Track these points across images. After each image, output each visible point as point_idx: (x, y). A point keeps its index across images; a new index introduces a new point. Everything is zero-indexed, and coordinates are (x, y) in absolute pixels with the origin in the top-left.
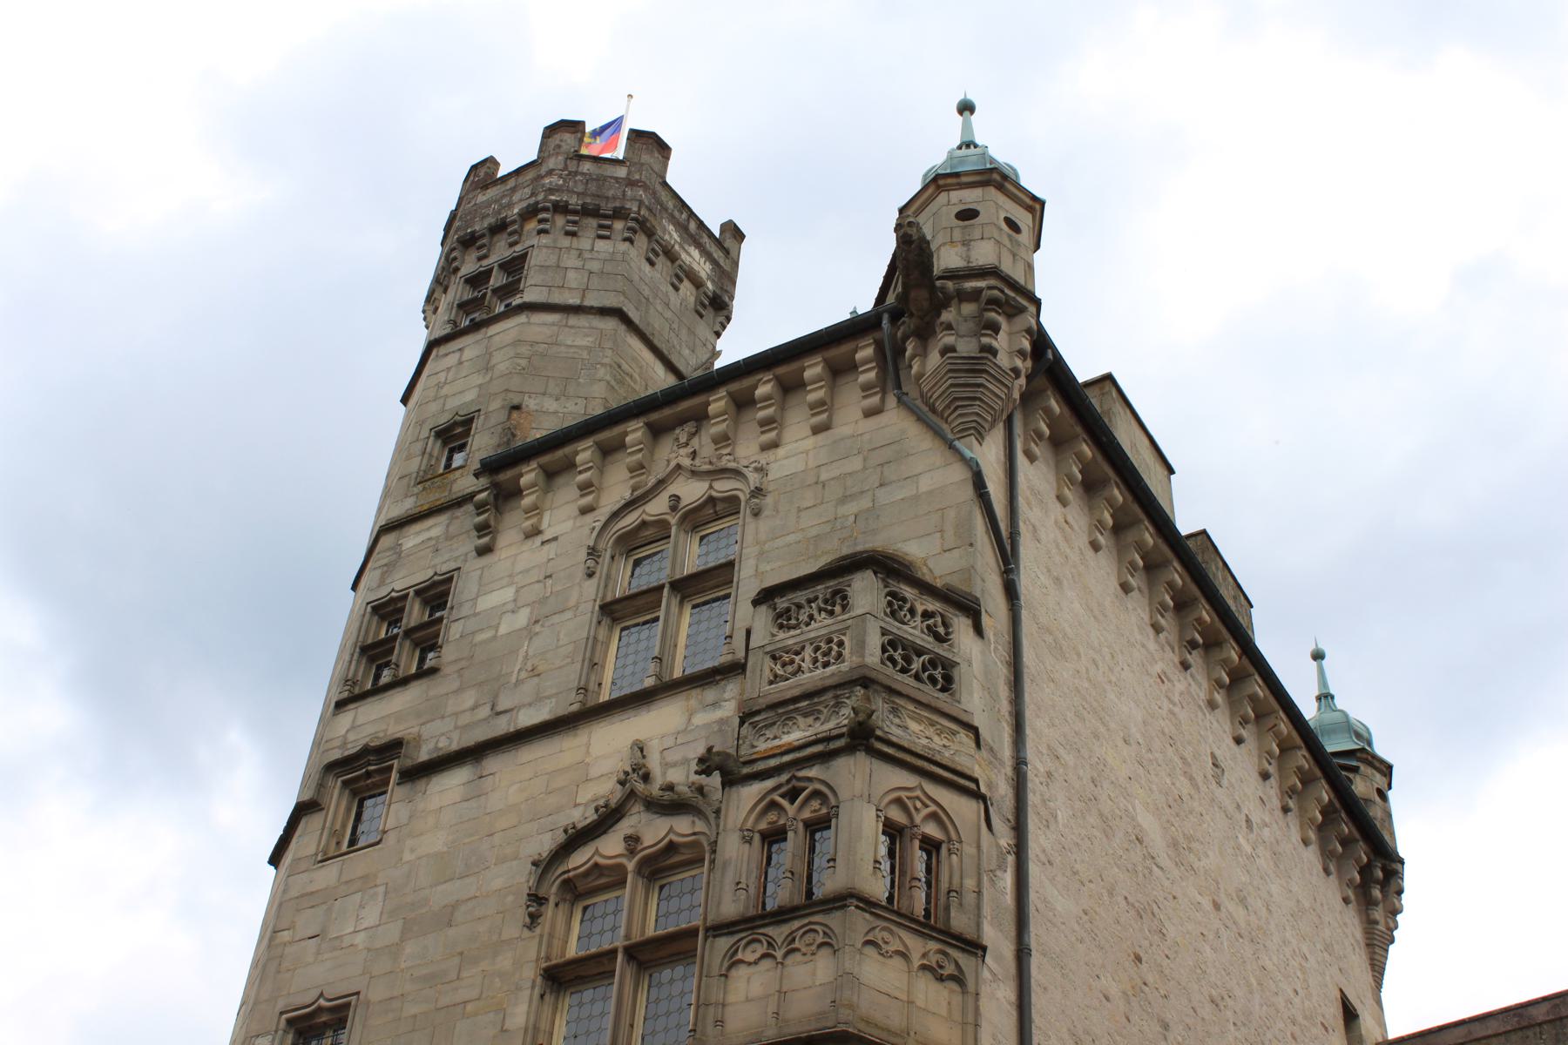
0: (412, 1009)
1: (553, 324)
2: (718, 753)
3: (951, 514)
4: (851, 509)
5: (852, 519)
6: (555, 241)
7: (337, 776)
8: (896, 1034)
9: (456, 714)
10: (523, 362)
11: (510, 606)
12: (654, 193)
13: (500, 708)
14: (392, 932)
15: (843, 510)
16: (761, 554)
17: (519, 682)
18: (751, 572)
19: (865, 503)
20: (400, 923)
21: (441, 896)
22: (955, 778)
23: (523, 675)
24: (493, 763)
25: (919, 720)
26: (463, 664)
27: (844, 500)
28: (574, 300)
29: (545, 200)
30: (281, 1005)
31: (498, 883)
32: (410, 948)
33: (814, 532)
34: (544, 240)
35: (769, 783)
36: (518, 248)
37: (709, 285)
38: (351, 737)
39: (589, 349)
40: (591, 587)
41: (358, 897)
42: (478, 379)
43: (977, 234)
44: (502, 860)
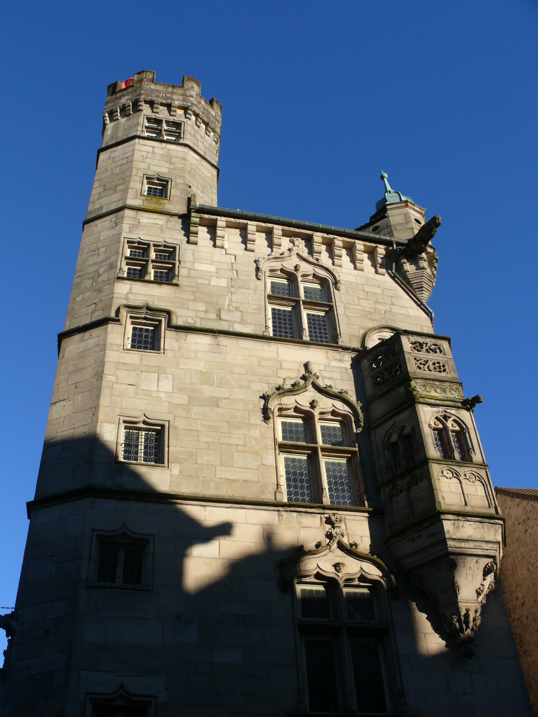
4: (383, 308)
5: (383, 312)
14: (183, 399)
15: (378, 306)
16: (345, 308)
18: (343, 313)
19: (387, 308)
21: (208, 391)
24: (224, 340)
26: (196, 290)
27: (377, 302)
30: (118, 411)
31: (241, 397)
33: (368, 310)
44: (242, 387)
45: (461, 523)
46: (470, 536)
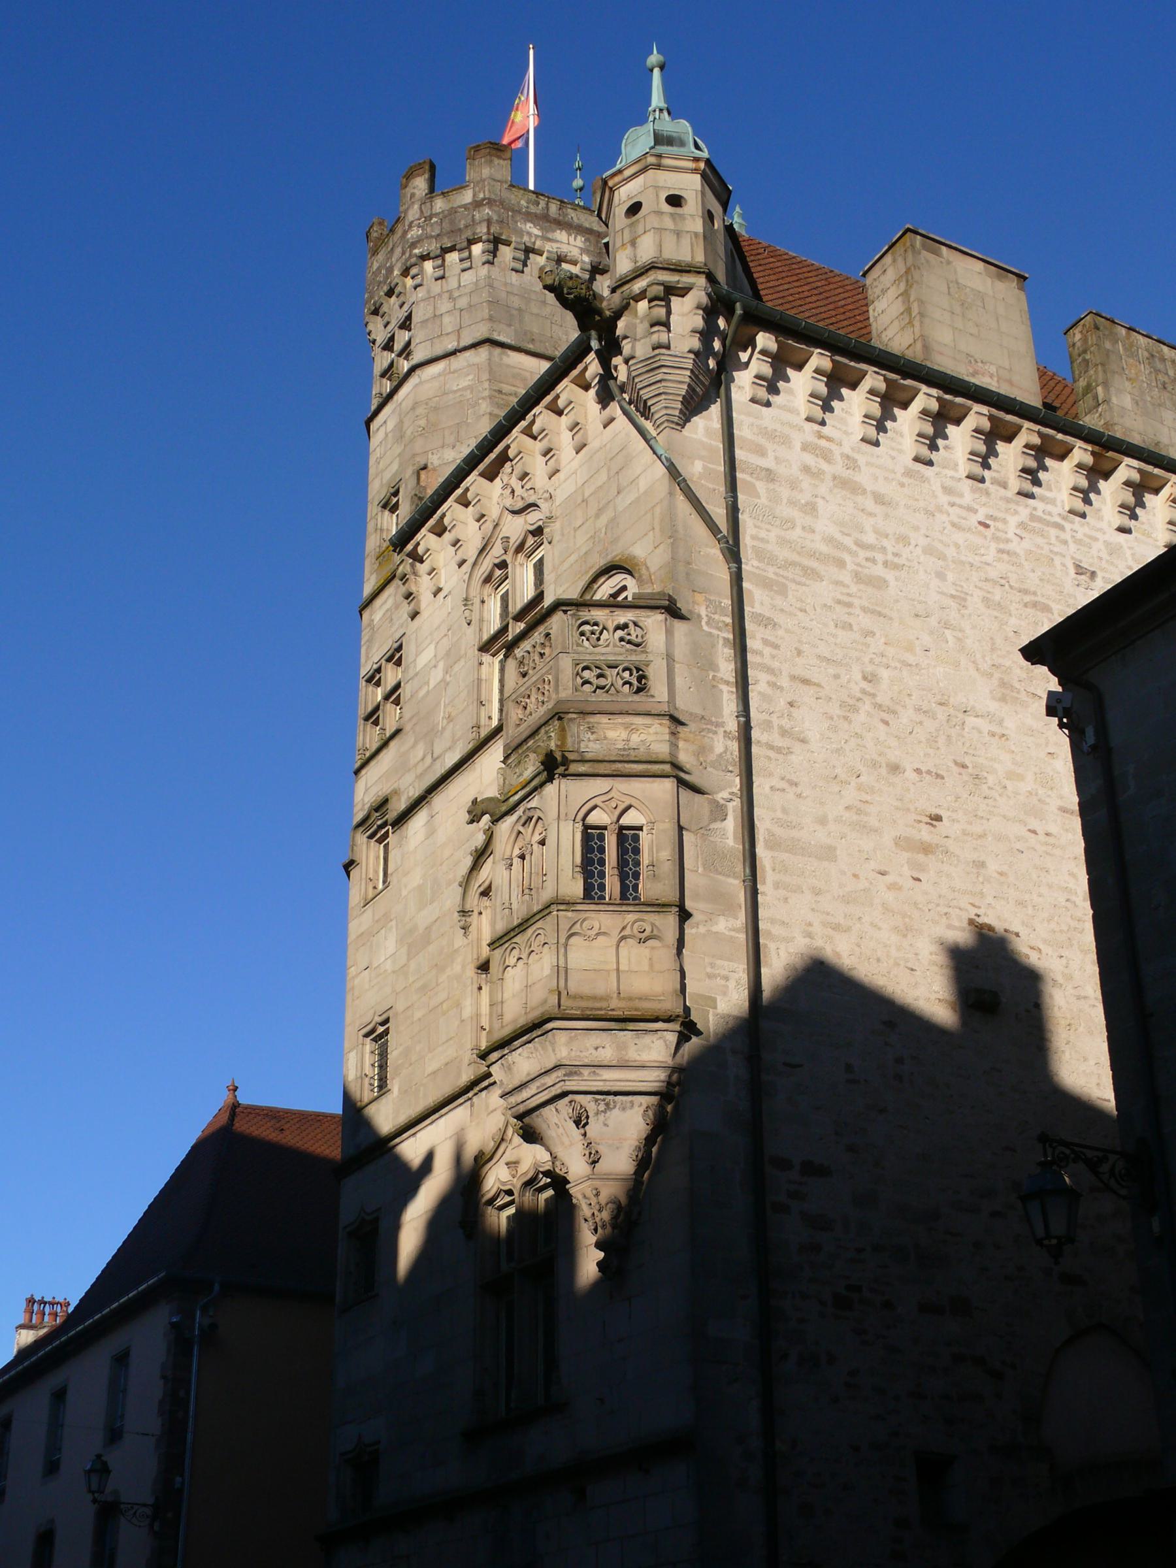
0: (418, 1014)
1: (439, 375)
2: (483, 801)
3: (658, 510)
4: (604, 520)
6: (429, 292)
7: (364, 832)
8: (602, 999)
9: (416, 765)
10: (423, 422)
11: (433, 662)
12: (502, 203)
13: (435, 755)
17: (444, 729)
20: (406, 947)
22: (649, 766)
23: (445, 721)
25: (614, 729)
28: (451, 345)
29: (411, 256)
32: (413, 965)
33: (584, 550)
34: (421, 293)
35: (514, 817)
36: (406, 307)
37: (586, 259)
38: (366, 800)
39: (470, 388)
40: (470, 631)
41: (383, 931)
42: (398, 449)
43: (640, 229)
45: (509, 1058)
46: (528, 1074)
